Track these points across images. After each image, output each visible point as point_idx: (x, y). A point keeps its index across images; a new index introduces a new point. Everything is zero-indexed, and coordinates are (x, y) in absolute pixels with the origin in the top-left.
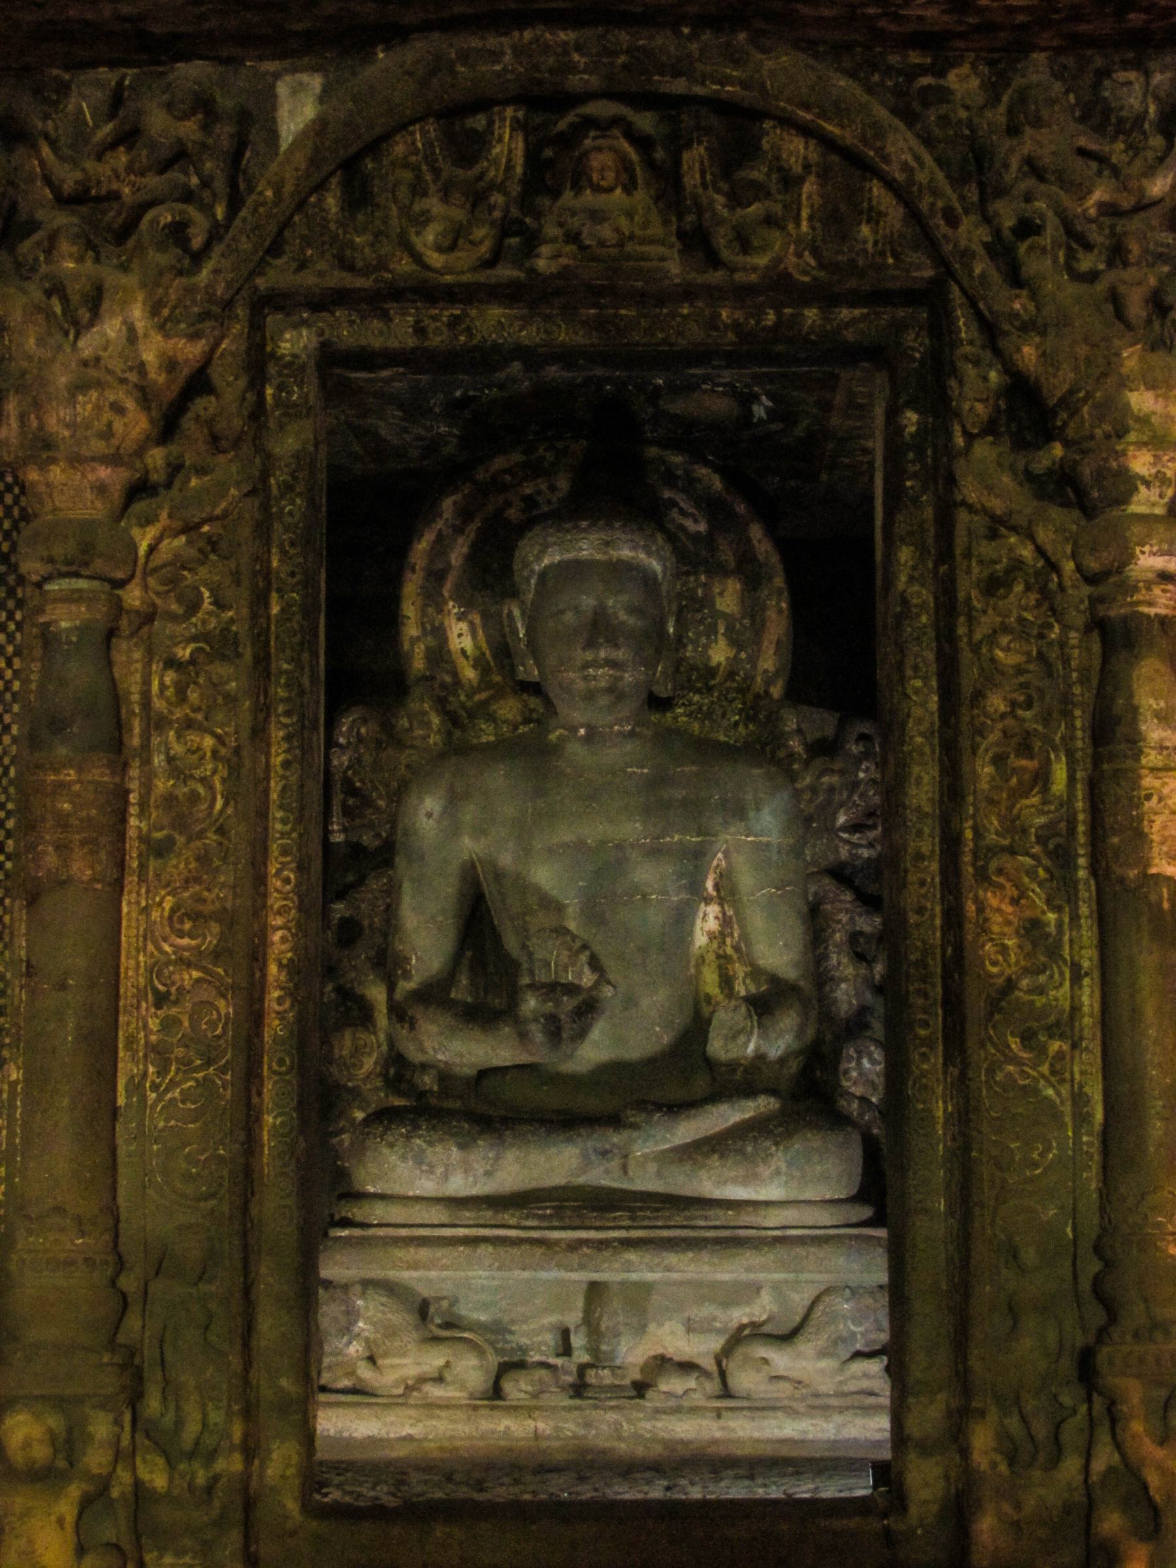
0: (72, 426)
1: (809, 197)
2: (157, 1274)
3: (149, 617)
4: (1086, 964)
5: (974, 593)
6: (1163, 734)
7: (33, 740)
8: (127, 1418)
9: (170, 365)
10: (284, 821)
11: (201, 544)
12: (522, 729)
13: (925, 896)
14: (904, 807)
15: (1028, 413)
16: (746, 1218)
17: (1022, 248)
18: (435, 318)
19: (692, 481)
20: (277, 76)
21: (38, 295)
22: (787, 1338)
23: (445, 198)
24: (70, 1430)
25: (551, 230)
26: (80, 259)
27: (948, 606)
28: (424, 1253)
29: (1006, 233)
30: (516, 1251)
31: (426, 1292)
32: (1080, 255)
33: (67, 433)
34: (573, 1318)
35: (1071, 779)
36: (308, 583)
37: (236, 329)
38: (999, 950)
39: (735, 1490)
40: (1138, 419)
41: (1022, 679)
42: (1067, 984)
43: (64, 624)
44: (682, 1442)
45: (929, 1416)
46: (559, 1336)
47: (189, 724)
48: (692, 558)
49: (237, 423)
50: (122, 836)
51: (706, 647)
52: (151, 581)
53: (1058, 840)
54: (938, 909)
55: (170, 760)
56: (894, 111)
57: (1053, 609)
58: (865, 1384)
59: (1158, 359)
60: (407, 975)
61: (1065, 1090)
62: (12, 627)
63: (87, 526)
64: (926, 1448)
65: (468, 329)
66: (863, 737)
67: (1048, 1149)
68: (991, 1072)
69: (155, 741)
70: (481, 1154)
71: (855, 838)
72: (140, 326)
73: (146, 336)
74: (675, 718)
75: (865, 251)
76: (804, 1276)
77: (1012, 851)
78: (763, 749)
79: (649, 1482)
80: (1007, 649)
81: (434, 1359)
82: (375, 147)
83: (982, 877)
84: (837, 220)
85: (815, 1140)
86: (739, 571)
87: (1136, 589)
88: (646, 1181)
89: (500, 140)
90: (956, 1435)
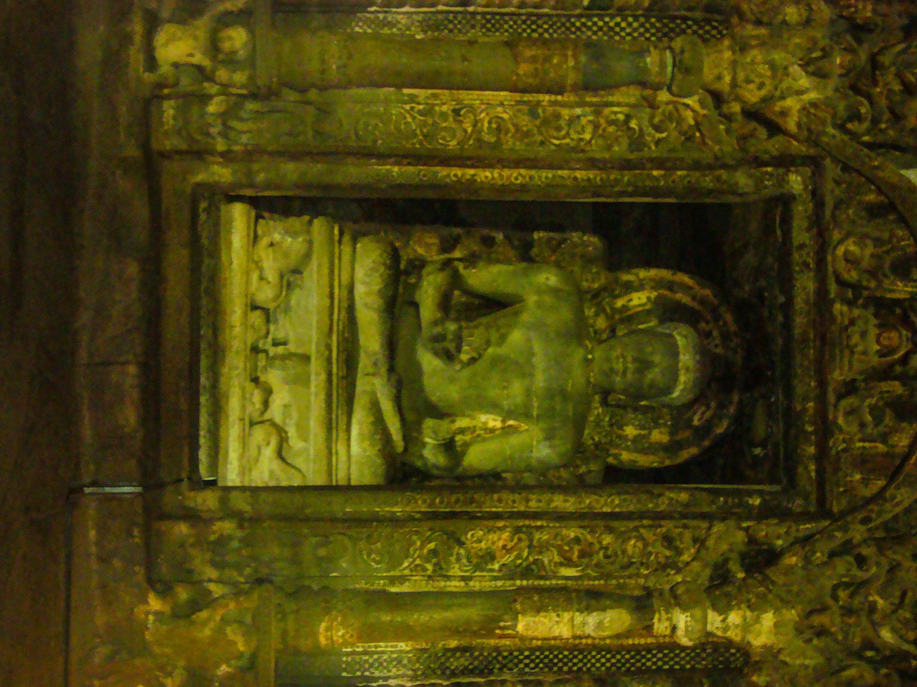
0: (753, 62)
2: (318, 109)
3: (653, 105)
4: (471, 583)
5: (664, 530)
6: (591, 625)
7: (589, 45)
8: (244, 92)
9: (784, 113)
10: (546, 178)
11: (689, 133)
12: (591, 329)
13: (507, 503)
14: (553, 494)
15: (759, 559)
16: (342, 435)
17: (850, 559)
18: (808, 254)
19: (720, 418)
21: (822, 43)
22: (280, 454)
23: (872, 256)
24: (238, 62)
25: (856, 312)
26: (841, 66)
27: (659, 517)
28: (325, 271)
30: (326, 319)
31: (305, 274)
32: (848, 592)
33: (748, 60)
34: (292, 348)
36: (669, 192)
37: (804, 149)
38: (479, 539)
39: (204, 420)
40: (758, 617)
41: (619, 553)
42: (462, 574)
43: (648, 60)
44: (227, 401)
45: (241, 503)
46: (282, 341)
47: (596, 126)
48: (680, 413)
49: (752, 149)
50: (539, 92)
51: (633, 425)
52: (671, 107)
53: (536, 572)
54: (501, 510)
55: (578, 117)
57: (656, 570)
59: (789, 629)
60: (465, 268)
61: (407, 572)
62: (648, 35)
63: (700, 70)
64: (224, 501)
65: (802, 271)
67: (377, 563)
68: (417, 532)
69: (587, 109)
70: (377, 302)
72: (806, 97)
73: (800, 100)
74: (596, 408)
75: (846, 476)
76: (311, 465)
77: (530, 547)
78: (579, 449)
79: (208, 379)
80: (635, 546)
81: (272, 276)
82: (903, 221)
83: (518, 530)
84: (863, 461)
85: (381, 470)
87: (667, 613)
88: (362, 384)
89: (906, 286)
90: (229, 513)
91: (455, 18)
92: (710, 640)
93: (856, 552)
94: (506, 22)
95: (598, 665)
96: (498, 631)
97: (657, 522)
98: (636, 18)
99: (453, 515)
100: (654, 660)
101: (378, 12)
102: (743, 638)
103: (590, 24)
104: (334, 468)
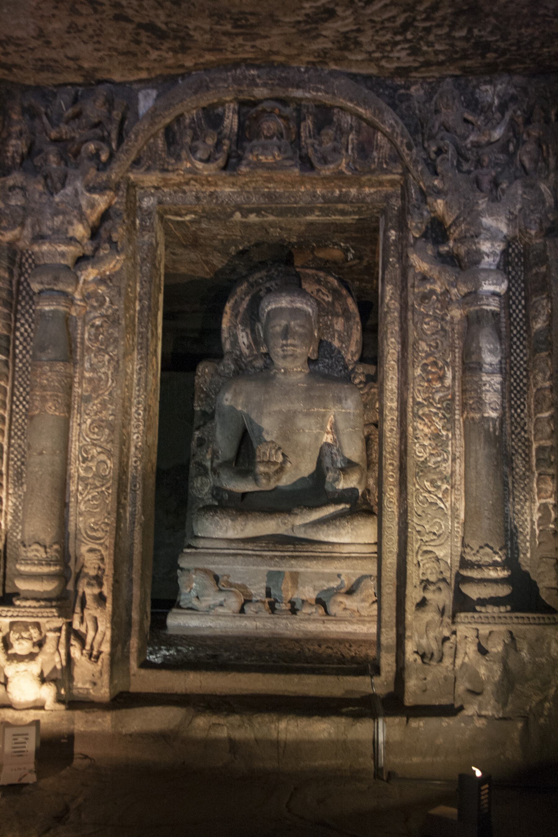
1: (352, 140)
4: (458, 454)
16: (337, 549)
20: (139, 90)
27: (404, 307)
28: (217, 559)
29: (433, 156)
30: (251, 559)
35: (454, 378)
40: (485, 229)
55: (91, 365)
56: (389, 104)
81: (220, 598)
86: (343, 315)
87: (482, 299)
88: (300, 534)
89: (228, 118)
91: (12, 460)
92: (502, 267)
93: (433, 156)
94: (17, 420)
95: (522, 355)
96: (497, 433)
97: (410, 308)
98: (16, 320)
99: (402, 469)
100: (517, 311)
101: (6, 519)
102: (502, 241)
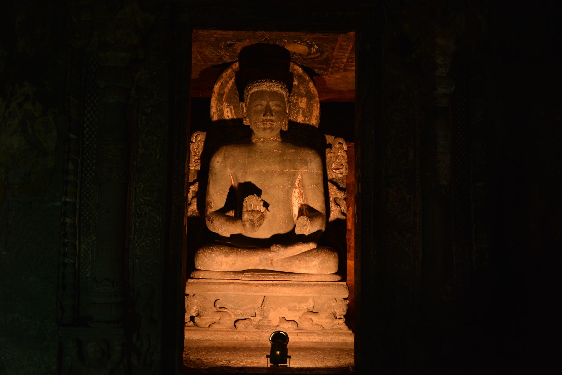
51: (296, 117)
58: (339, 326)
62: (95, 101)
66: (340, 143)
71: (337, 171)
86: (306, 96)
103: (87, 136)
104: (325, 283)
